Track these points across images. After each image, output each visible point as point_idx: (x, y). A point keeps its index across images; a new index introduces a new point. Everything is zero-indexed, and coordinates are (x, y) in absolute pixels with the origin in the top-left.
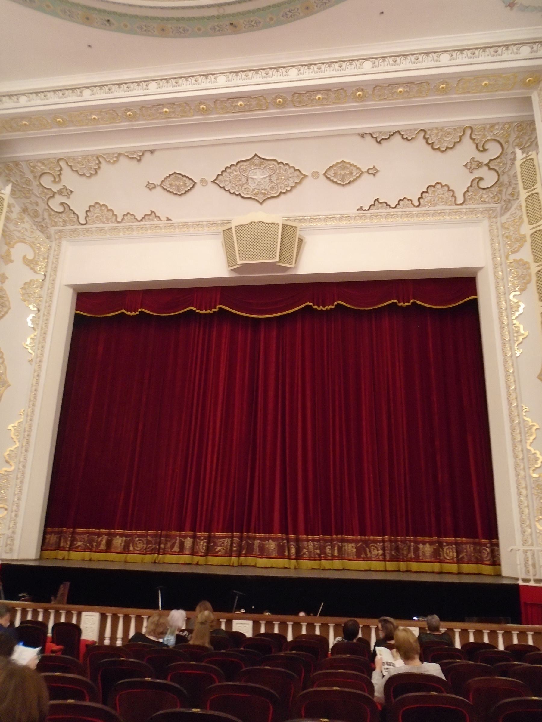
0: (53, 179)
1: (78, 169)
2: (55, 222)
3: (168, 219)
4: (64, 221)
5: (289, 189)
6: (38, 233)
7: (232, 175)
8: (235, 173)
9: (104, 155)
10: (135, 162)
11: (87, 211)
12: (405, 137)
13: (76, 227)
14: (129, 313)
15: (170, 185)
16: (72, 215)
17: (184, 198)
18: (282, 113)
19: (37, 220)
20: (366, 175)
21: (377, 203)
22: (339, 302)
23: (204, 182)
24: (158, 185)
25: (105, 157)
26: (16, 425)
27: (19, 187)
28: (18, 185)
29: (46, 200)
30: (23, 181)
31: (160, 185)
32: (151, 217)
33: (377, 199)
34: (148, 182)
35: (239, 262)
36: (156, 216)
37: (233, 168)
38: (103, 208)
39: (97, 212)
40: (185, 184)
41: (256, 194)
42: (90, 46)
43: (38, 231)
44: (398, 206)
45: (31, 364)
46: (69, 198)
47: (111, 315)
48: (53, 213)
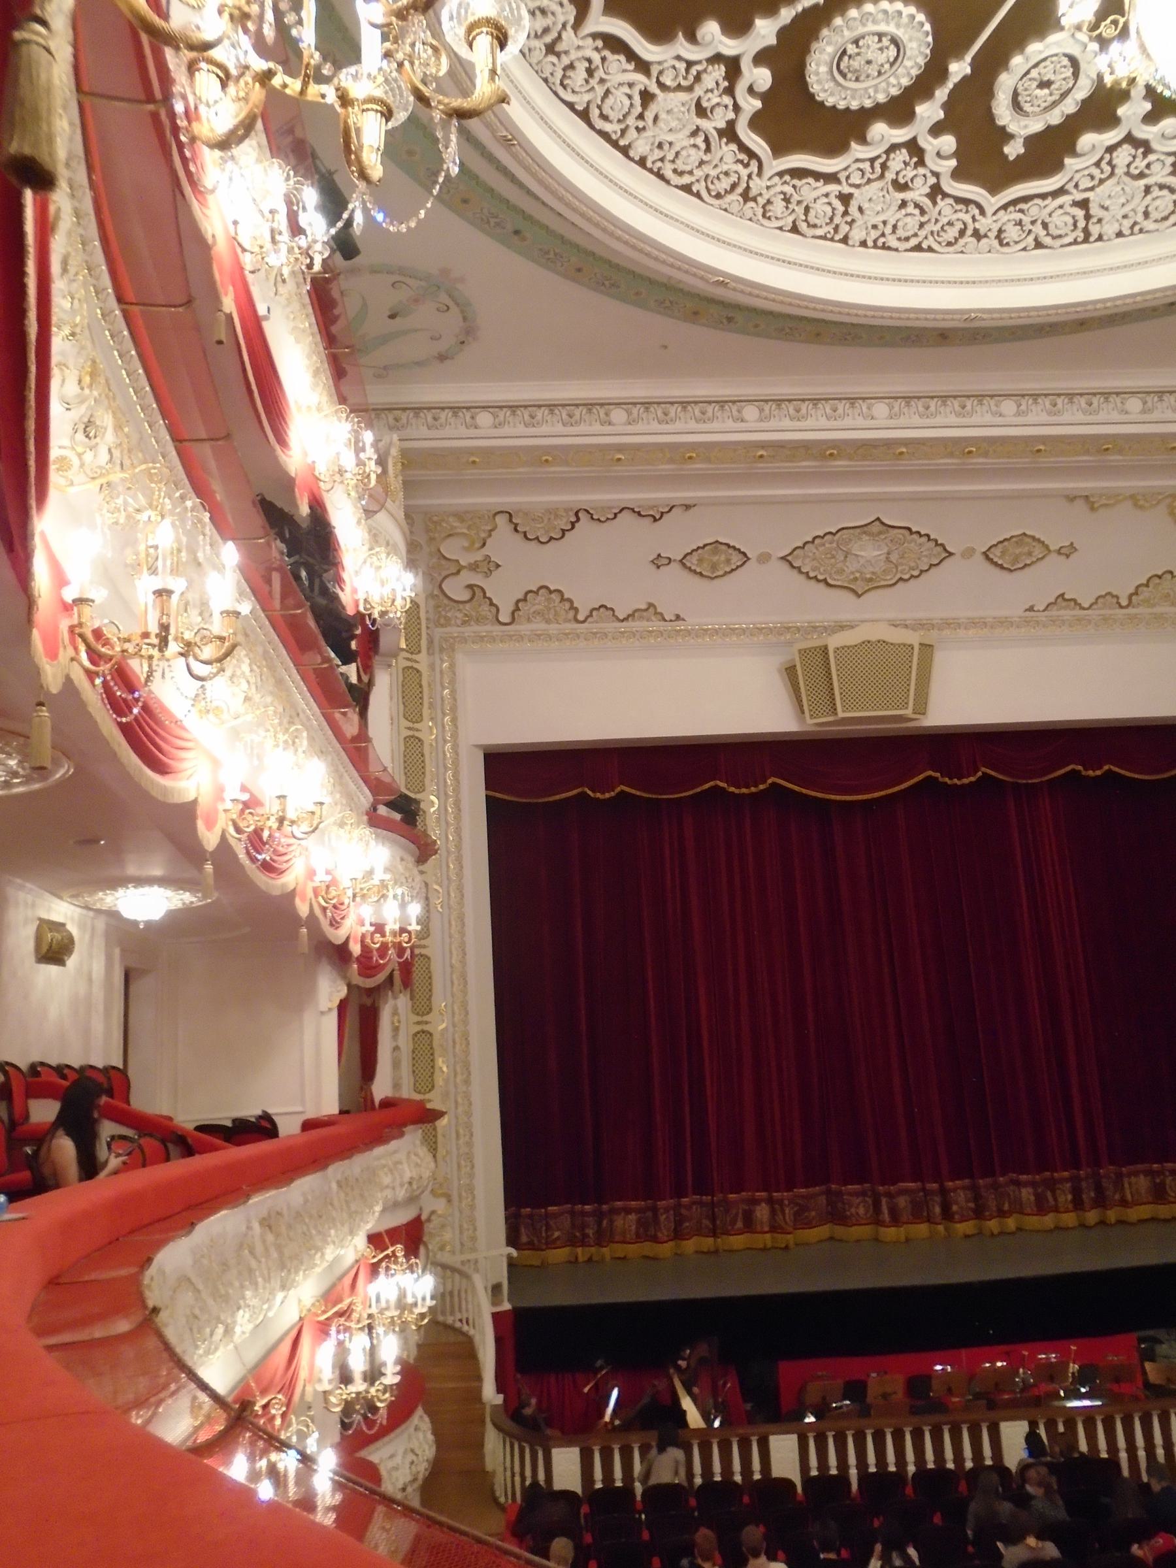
0: (466, 544)
1: (527, 529)
2: (448, 619)
3: (678, 617)
4: (466, 615)
5: (916, 573)
7: (821, 549)
8: (827, 545)
11: (518, 601)
12: (1141, 503)
13: (489, 628)
14: (598, 795)
15: (700, 561)
16: (486, 607)
17: (715, 582)
18: (964, 464)
20: (1054, 556)
21: (1060, 600)
22: (983, 769)
23: (764, 558)
29: (439, 579)
31: (681, 561)
32: (645, 614)
33: (1062, 595)
34: (659, 555)
35: (841, 715)
36: (656, 613)
37: (827, 537)
38: (553, 596)
39: (540, 601)
40: (728, 561)
41: (856, 579)
42: (666, 347)
44: (1095, 607)
47: (557, 797)
48: (446, 601)
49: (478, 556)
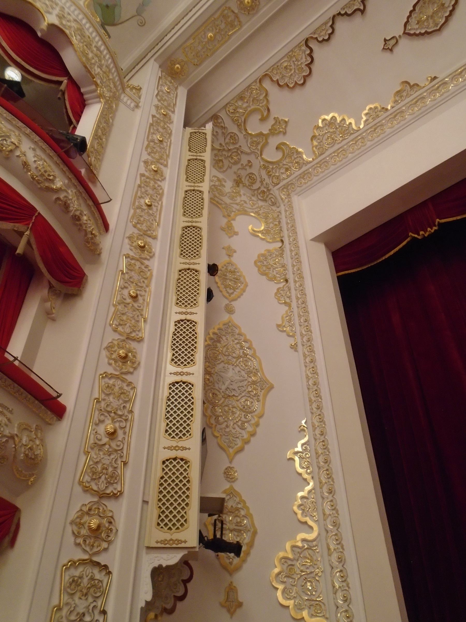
1: (286, 80)
2: (278, 177)
6: (261, 203)
9: (314, 33)
10: (358, 18)
19: (255, 186)
24: (400, 36)
25: (315, 36)
26: (299, 449)
27: (224, 153)
28: (224, 150)
30: (227, 140)
31: (404, 33)
34: (385, 40)
43: (259, 202)
45: (296, 351)
46: (285, 133)
47: (392, 253)
49: (271, 122)
